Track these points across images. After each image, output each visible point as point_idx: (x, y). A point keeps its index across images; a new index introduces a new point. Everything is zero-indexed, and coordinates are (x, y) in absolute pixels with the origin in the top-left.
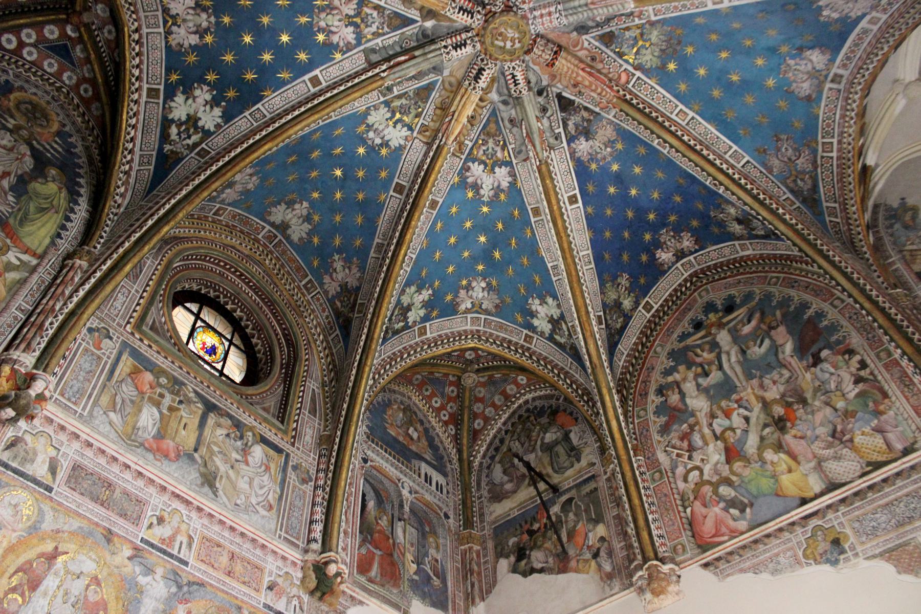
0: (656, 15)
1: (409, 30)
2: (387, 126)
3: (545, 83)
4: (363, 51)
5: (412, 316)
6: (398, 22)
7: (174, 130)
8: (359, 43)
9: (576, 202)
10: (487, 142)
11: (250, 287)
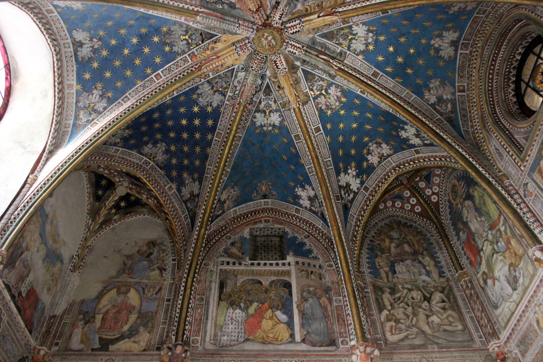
1: (308, 69)
2: (359, 37)
4: (334, 79)
6: (310, 77)
7: (426, 142)
8: (333, 83)
11: (499, 51)
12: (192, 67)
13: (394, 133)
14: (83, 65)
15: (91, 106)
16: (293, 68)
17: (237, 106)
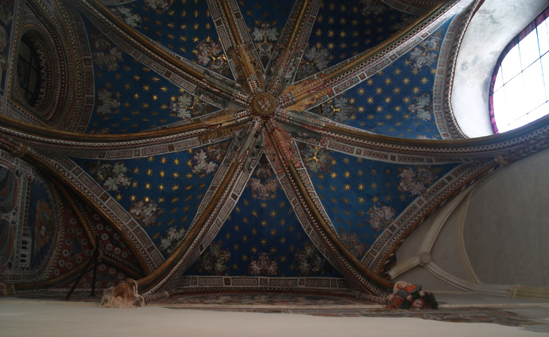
0: (329, 146)
2: (184, 108)
3: (262, 145)
4: (205, 70)
5: (109, 182)
7: (115, 10)
8: (206, 67)
9: (235, 199)
10: (217, 149)
11: (60, 96)
12: (332, 84)
13: (146, 19)
14: (427, 90)
15: (425, 53)
16: (243, 81)
17: (293, 47)
